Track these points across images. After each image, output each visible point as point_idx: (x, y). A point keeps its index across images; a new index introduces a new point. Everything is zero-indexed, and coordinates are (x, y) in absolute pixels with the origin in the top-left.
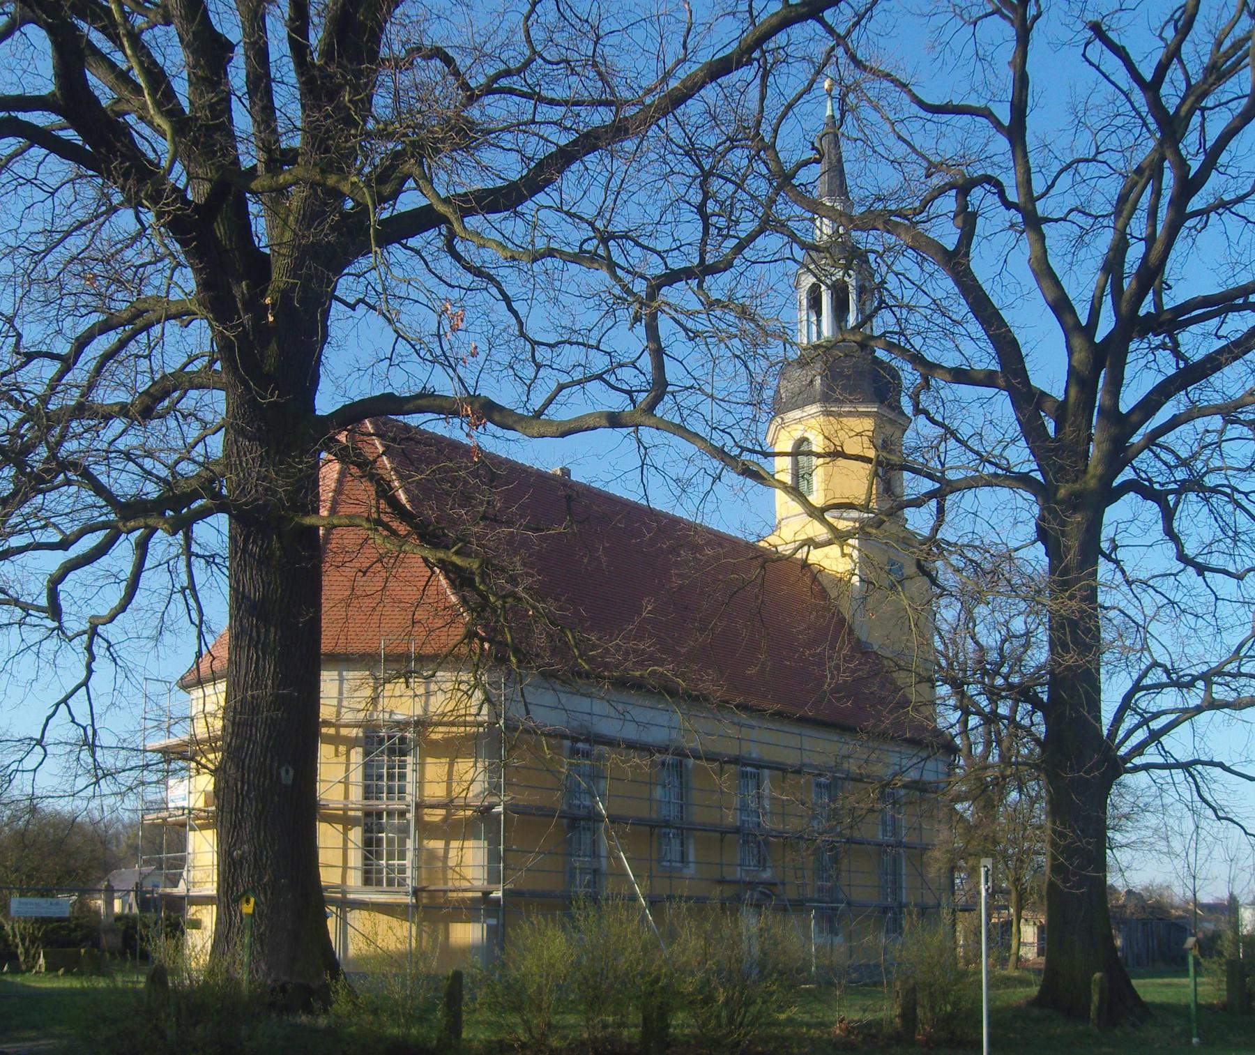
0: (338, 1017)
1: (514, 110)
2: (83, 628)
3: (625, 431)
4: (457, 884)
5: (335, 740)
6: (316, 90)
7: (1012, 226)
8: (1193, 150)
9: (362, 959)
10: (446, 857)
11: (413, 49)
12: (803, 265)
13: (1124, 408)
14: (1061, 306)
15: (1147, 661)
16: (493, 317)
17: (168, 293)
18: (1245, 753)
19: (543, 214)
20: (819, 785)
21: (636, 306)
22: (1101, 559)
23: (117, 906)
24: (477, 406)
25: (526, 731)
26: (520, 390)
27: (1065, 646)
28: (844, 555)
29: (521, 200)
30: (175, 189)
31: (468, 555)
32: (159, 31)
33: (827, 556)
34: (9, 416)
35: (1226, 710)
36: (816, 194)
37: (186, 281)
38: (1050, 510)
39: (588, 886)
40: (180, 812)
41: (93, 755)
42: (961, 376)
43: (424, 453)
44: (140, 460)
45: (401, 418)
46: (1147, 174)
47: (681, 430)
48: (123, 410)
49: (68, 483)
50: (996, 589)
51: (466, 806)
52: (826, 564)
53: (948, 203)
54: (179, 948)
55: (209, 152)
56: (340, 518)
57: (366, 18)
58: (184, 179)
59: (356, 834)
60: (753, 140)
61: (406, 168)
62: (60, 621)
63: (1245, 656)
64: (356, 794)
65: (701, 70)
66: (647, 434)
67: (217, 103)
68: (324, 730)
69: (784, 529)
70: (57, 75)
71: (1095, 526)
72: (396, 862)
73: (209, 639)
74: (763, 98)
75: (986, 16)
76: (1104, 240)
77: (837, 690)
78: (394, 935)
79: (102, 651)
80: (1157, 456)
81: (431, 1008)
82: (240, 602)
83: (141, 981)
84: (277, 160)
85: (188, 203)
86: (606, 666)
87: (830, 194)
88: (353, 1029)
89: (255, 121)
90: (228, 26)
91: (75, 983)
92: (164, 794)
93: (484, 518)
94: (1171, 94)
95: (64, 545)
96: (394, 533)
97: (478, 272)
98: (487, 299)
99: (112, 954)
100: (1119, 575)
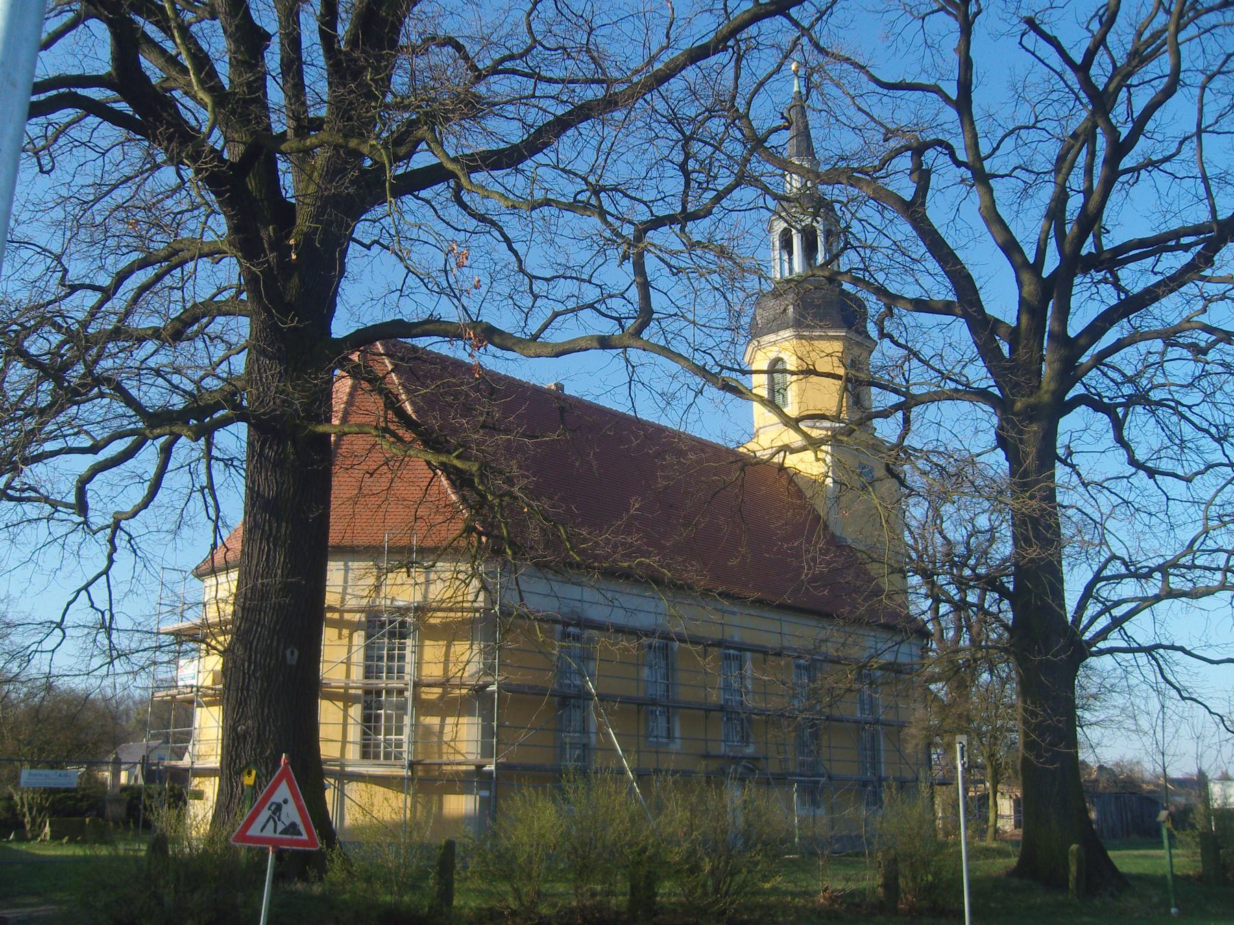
0: (333, 884)
1: (516, 87)
2: (107, 523)
3: (614, 352)
4: (452, 758)
5: (339, 624)
6: (341, 68)
7: (963, 181)
8: (1122, 119)
9: (358, 829)
10: (441, 732)
11: (428, 39)
12: (774, 213)
13: (1072, 333)
14: (1010, 247)
15: (1105, 555)
16: (495, 256)
17: (202, 235)
18: (1204, 638)
19: (541, 170)
20: (798, 667)
21: (625, 246)
22: (1058, 464)
23: (124, 778)
24: (479, 330)
25: (521, 616)
26: (518, 317)
27: (1027, 541)
28: (818, 460)
29: (522, 159)
30: (213, 150)
31: (468, 459)
32: (206, 24)
33: (802, 461)
34: (51, 338)
35: (1184, 599)
36: (785, 154)
37: (219, 225)
38: (1008, 421)
39: (578, 759)
40: (189, 690)
41: (109, 637)
42: (921, 305)
43: (430, 371)
44: (168, 376)
45: (409, 340)
46: (1082, 138)
47: (666, 351)
48: (156, 333)
49: (102, 395)
50: (961, 490)
51: (461, 685)
52: (801, 467)
53: (904, 162)
54: (181, 818)
55: (245, 120)
56: (350, 426)
57: (388, 14)
58: (221, 142)
59: (356, 711)
60: (728, 111)
61: (419, 133)
62: (86, 516)
63: (1198, 550)
64: (357, 673)
65: (682, 55)
66: (634, 354)
67: (254, 81)
68: (329, 615)
69: (761, 437)
70: (114, 59)
71: (1050, 435)
72: (393, 737)
73: (225, 533)
74: (737, 77)
75: (933, 12)
76: (1047, 193)
77: (814, 579)
78: (389, 806)
79: (124, 543)
80: (1105, 374)
81: (424, 875)
82: (255, 500)
83: (142, 849)
84: (304, 127)
85: (224, 161)
86: (596, 558)
87: (799, 154)
88: (347, 896)
89: (287, 95)
90: (266, 20)
91: (78, 851)
92: (174, 673)
93: (484, 426)
94: (1100, 74)
95: (94, 449)
96: (400, 439)
97: (482, 218)
98: (490, 241)
99: (116, 823)
100: (1075, 477)
